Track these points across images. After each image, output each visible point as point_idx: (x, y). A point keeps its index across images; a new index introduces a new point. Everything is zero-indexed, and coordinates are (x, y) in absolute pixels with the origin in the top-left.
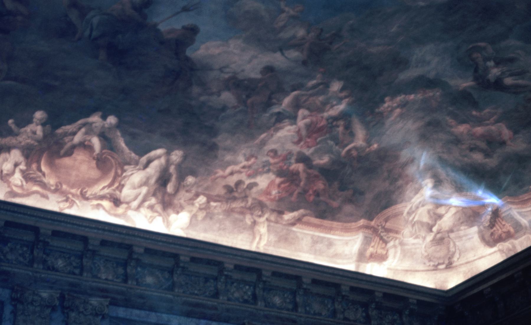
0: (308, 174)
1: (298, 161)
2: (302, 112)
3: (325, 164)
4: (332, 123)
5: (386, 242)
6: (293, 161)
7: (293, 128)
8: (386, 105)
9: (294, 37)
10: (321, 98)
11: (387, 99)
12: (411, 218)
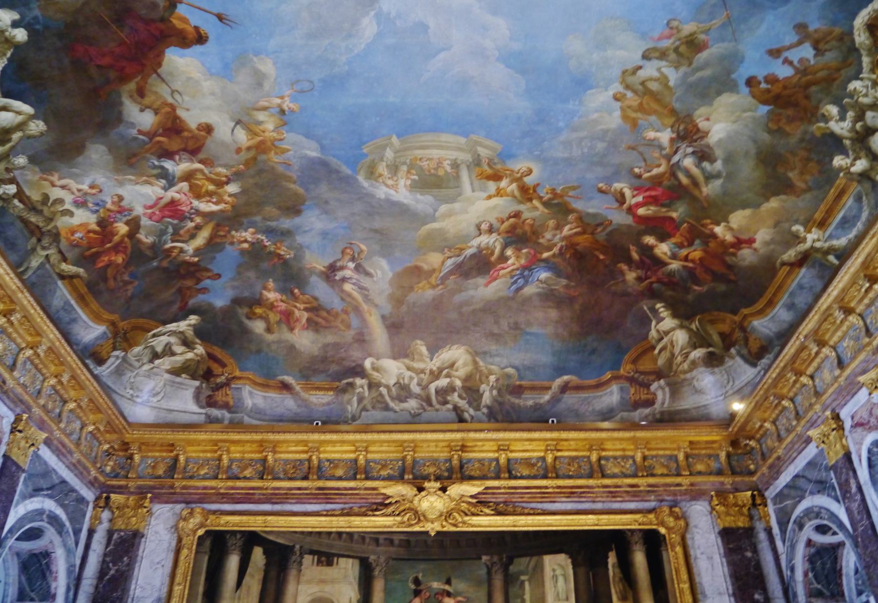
0: (122, 241)
1: (127, 223)
2: (184, 185)
6: (125, 219)
7: (160, 192)
8: (244, 234)
9: (260, 123)
10: (211, 187)
11: (251, 230)
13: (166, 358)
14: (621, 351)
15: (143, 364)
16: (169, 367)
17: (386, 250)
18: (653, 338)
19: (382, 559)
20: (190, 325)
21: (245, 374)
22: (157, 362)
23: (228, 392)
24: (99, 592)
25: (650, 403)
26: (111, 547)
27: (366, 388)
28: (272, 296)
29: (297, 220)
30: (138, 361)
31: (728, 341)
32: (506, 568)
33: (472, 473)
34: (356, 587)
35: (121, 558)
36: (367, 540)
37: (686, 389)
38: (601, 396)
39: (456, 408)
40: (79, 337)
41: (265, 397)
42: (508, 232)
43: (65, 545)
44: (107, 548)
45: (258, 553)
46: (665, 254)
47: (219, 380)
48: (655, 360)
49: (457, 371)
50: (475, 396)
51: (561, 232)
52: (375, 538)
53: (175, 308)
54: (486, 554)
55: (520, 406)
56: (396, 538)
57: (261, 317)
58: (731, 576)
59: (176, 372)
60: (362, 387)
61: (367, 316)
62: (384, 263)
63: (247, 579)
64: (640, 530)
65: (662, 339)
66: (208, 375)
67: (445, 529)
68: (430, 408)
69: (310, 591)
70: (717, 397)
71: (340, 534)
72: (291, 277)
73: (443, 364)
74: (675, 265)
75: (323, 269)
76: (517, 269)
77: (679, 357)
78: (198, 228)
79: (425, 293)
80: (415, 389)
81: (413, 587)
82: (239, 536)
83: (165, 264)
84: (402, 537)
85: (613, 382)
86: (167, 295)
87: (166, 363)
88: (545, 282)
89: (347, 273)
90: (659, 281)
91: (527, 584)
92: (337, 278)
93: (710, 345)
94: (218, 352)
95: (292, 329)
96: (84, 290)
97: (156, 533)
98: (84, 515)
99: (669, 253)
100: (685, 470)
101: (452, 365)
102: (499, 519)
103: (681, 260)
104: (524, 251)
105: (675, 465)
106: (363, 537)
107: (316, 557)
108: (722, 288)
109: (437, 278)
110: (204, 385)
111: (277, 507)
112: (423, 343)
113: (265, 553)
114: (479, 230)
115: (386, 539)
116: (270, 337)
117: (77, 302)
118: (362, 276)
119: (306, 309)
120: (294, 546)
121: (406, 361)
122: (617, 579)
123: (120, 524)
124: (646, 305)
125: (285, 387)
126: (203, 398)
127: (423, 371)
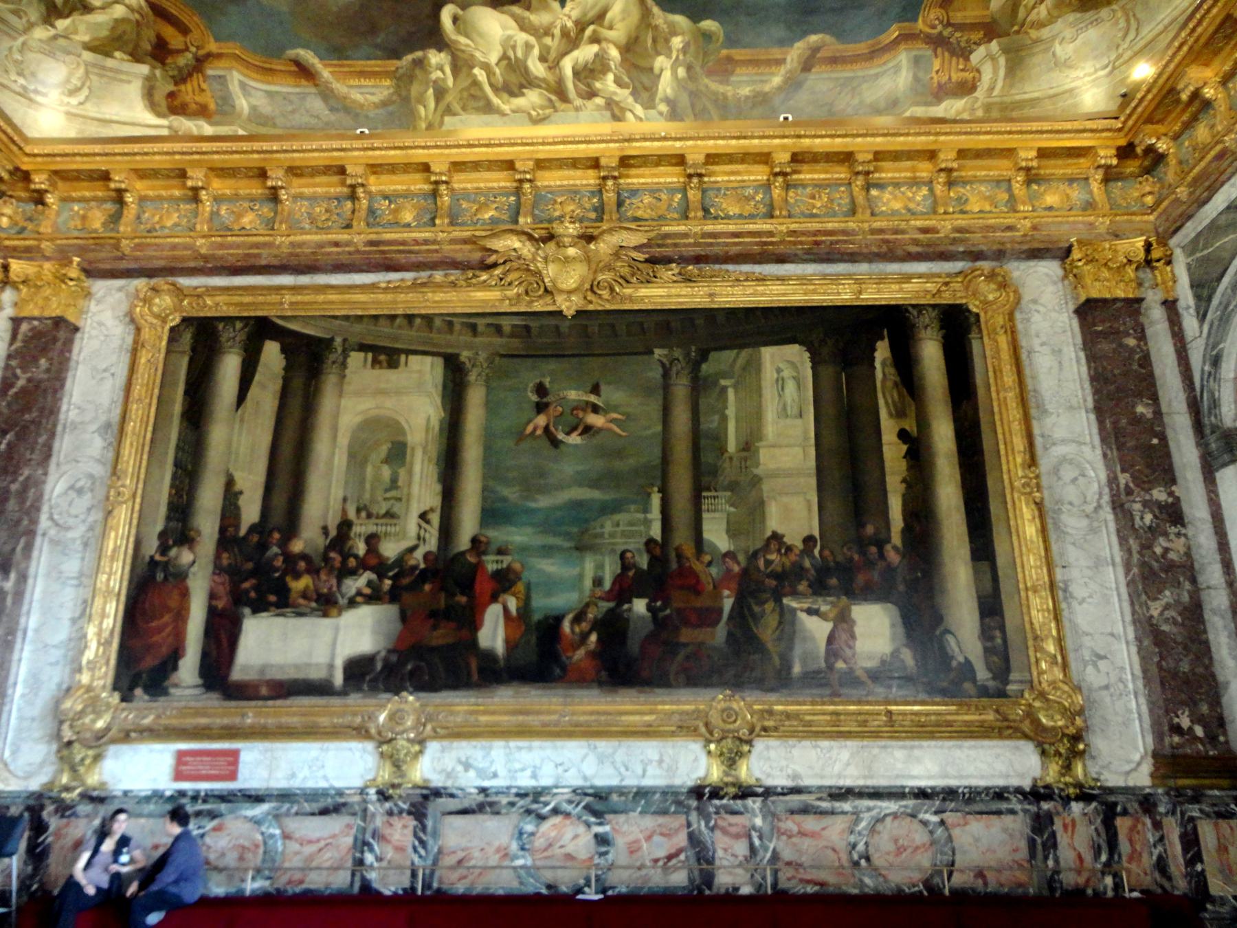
13: (76, 17)
16: (86, 38)
19: (483, 356)
22: (62, 24)
23: (204, 86)
25: (966, 88)
27: (448, 70)
30: (16, 13)
32: (696, 366)
33: (639, 213)
34: (438, 401)
35: (35, 360)
36: (457, 327)
37: (1037, 59)
38: (877, 76)
39: (610, 104)
41: (270, 94)
44: (11, 344)
45: (272, 352)
47: (184, 60)
49: (611, 28)
50: (645, 79)
52: (471, 322)
54: (662, 347)
55: (725, 98)
56: (506, 323)
59: (102, 48)
60: (442, 69)
64: (934, 306)
66: (160, 52)
67: (591, 307)
68: (564, 106)
70: (1096, 71)
71: (410, 318)
73: (585, 14)
80: (537, 68)
81: (535, 398)
82: (239, 325)
84: (517, 321)
85: (902, 46)
91: (731, 393)
97: (100, 324)
100: (1024, 203)
101: (600, 18)
105: (1006, 196)
106: (449, 321)
107: (370, 355)
110: (158, 72)
111: (304, 280)
113: (283, 350)
120: (332, 339)
121: (516, 9)
122: (889, 384)
123: (32, 310)
125: (304, 71)
126: (160, 96)
127: (548, 32)
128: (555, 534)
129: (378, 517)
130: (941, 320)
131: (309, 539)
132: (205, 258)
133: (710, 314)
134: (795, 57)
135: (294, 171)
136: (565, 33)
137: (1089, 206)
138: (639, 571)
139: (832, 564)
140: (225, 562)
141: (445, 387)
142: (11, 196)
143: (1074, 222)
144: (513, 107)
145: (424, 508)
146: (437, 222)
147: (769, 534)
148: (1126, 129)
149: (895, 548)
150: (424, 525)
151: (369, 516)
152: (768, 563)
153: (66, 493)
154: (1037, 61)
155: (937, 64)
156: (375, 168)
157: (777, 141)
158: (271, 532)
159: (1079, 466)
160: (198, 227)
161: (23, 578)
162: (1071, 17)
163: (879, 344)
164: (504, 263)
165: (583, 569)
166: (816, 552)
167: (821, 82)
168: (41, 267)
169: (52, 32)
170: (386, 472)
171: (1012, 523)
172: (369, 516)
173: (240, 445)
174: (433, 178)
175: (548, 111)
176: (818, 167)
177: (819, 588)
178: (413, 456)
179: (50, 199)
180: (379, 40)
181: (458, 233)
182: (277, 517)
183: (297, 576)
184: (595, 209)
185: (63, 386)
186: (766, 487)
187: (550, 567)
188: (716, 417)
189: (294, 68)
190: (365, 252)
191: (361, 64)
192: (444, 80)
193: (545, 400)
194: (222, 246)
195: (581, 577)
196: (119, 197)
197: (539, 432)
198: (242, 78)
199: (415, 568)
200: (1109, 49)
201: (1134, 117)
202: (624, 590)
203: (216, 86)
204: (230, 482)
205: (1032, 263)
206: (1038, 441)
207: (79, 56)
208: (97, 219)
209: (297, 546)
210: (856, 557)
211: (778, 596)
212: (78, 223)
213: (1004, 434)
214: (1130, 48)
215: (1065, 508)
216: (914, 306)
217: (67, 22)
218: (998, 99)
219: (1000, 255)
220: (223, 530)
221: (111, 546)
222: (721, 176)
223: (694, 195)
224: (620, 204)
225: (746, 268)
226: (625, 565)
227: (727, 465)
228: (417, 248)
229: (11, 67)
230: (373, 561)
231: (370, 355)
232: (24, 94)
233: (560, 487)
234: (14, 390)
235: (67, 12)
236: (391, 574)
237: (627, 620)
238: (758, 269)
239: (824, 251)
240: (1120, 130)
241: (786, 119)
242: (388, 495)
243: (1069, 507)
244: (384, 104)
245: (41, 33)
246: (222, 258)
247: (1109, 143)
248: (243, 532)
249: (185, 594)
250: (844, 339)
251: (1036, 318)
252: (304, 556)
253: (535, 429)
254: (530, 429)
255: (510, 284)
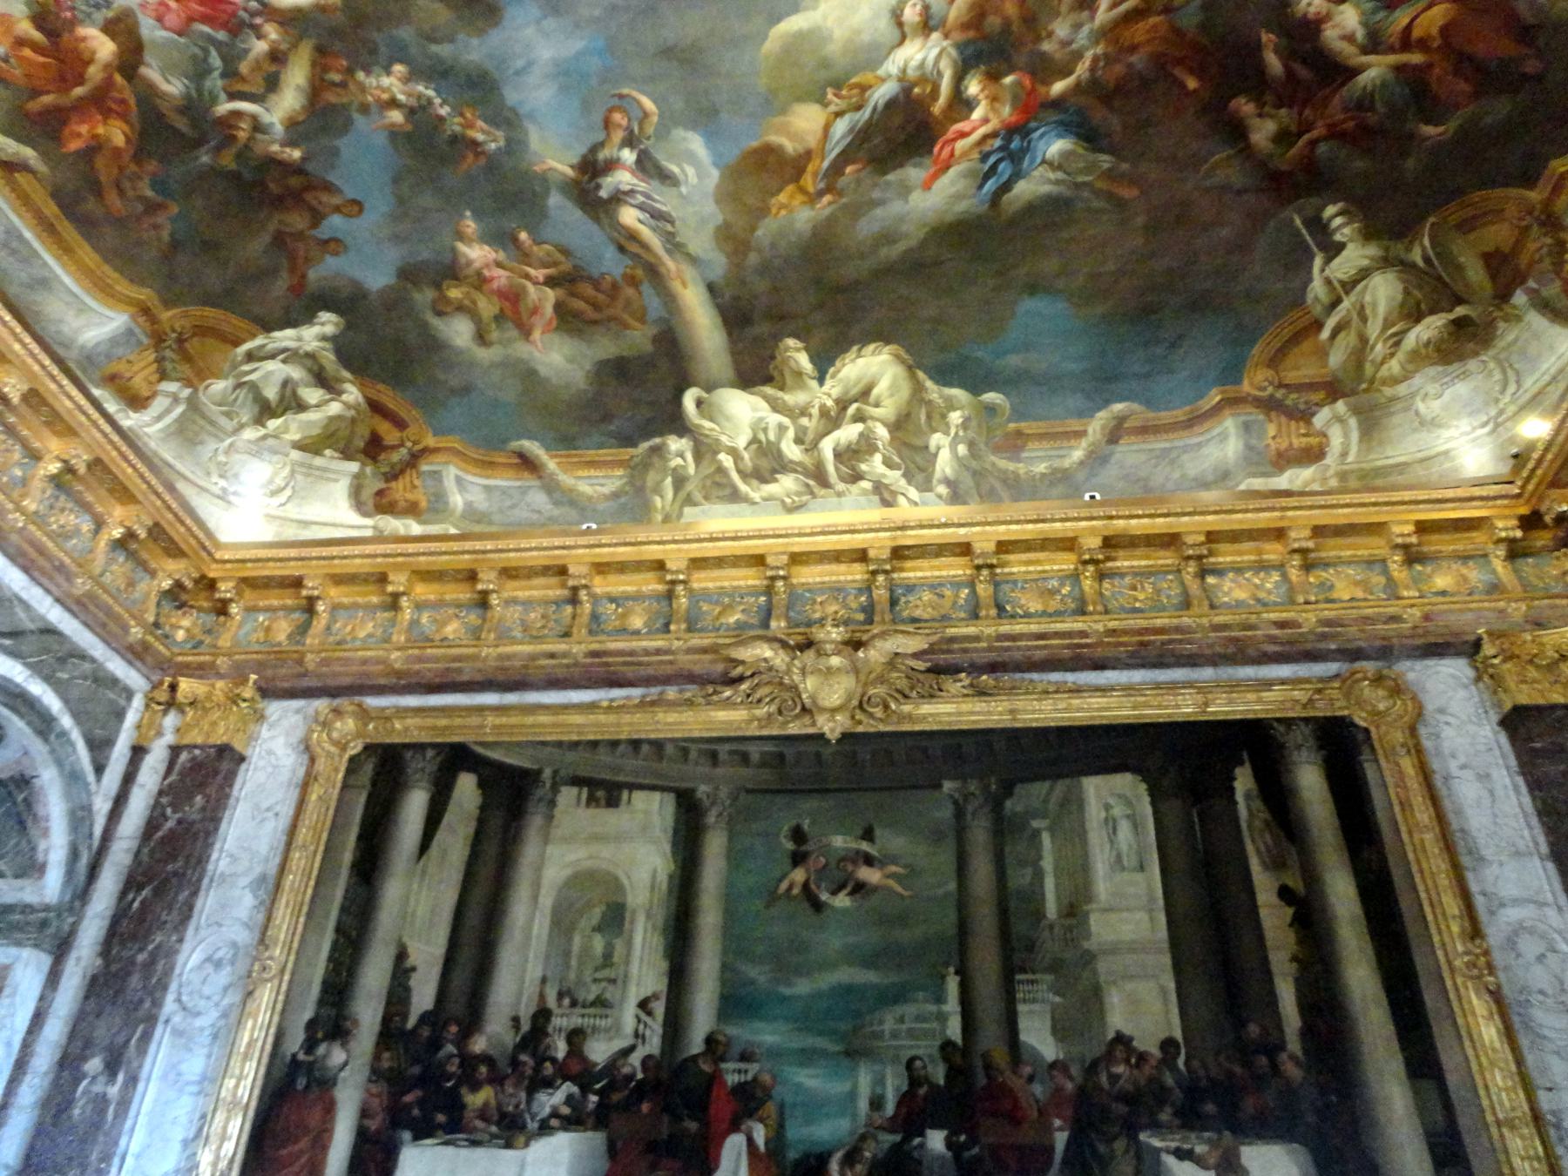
0: (108, 84)
1: (109, 28)
3: (163, 96)
4: (253, 14)
5: (163, 376)
8: (386, 81)
11: (399, 68)
12: (246, 368)
13: (289, 416)
14: (1243, 338)
15: (242, 427)
16: (297, 437)
17: (704, 117)
18: (1316, 299)
19: (724, 792)
20: (324, 338)
21: (444, 443)
22: (273, 424)
23: (416, 482)
24: (140, 863)
25: (1313, 455)
26: (173, 778)
27: (689, 456)
28: (477, 254)
29: (495, 37)
30: (228, 415)
31: (1506, 273)
33: (918, 613)
34: (667, 848)
35: (190, 797)
36: (693, 755)
37: (1396, 420)
38: (1200, 445)
40: (65, 329)
41: (487, 488)
42: (965, 26)
43: (59, 763)
45: (466, 787)
46: (1350, 38)
47: (396, 457)
48: (1322, 353)
49: (877, 405)
51: (1092, 18)
52: (712, 750)
53: (282, 284)
56: (755, 751)
57: (460, 308)
58: (1540, 814)
59: (310, 446)
60: (681, 455)
61: (676, 286)
62: (696, 143)
63: (441, 836)
64: (1306, 720)
65: (1336, 302)
66: (373, 448)
67: (860, 729)
68: (823, 492)
69: (572, 857)
70: (1474, 429)
71: (636, 744)
72: (510, 196)
73: (846, 393)
74: (1375, 71)
75: (570, 172)
76: (993, 135)
77: (1379, 347)
78: (277, 57)
79: (796, 214)
80: (792, 451)
81: (790, 846)
83: (228, 161)
84: (769, 748)
85: (1227, 412)
86: (255, 247)
87: (293, 427)
88: (1059, 167)
89: (623, 178)
90: (1334, 134)
91: (1046, 839)
92: (603, 194)
93: (1459, 301)
94: (388, 397)
95: (526, 333)
96: (51, 209)
97: (270, 752)
98: (120, 715)
99: (1360, 35)
100: (1407, 588)
101: (865, 394)
102: (979, 705)
103: (1392, 50)
104: (1008, 80)
105: (1383, 580)
106: (684, 747)
107: (585, 791)
108: (1499, 109)
109: (815, 174)
110: (368, 470)
111: (511, 698)
112: (800, 345)
113: (482, 784)
114: (900, 25)
115: (731, 753)
116: (483, 354)
117: (39, 237)
118: (655, 183)
119: (551, 282)
120: (539, 772)
121: (768, 390)
122: (1257, 823)
124: (1299, 212)
125: (527, 463)
126: (368, 493)
127: (804, 412)
128: (820, 1033)
129: (584, 1007)
130: (1318, 738)
131: (495, 1033)
132: (399, 674)
133: (1014, 737)
134: (1098, 428)
135: (508, 573)
136: (824, 412)
137: (1495, 588)
138: (933, 1087)
139: (1204, 1083)
140: (386, 1064)
141: (676, 831)
142: (192, 607)
143: (1480, 609)
144: (764, 494)
145: (646, 991)
146: (672, 627)
147: (1111, 1035)
148: (1526, 495)
149: (1292, 1057)
150: (643, 1016)
151: (574, 1004)
152: (1114, 1078)
153: (200, 967)
154: (1398, 421)
155: (1271, 430)
156: (601, 568)
157: (1084, 524)
158: (446, 1024)
159: (1543, 937)
160: (395, 638)
161: (133, 1080)
162: (1432, 371)
163: (1238, 771)
164: (752, 675)
165: (855, 1086)
166: (1181, 1062)
167: (1130, 454)
168: (213, 686)
169: (262, 432)
170: (598, 944)
171: (1460, 1021)
172: (574, 1004)
173: (418, 906)
174: (669, 577)
175: (805, 498)
176: (1138, 552)
177: (1190, 1119)
178: (632, 922)
179: (234, 609)
180: (612, 428)
181: (696, 641)
182: (457, 1007)
183: (475, 1087)
184: (863, 609)
185: (216, 829)
186: (1102, 966)
187: (809, 1079)
188: (1029, 871)
189: (517, 461)
190: (584, 666)
191: (591, 454)
192: (684, 467)
193: (803, 848)
194: (420, 660)
195: (852, 1096)
196: (309, 607)
197: (796, 891)
198: (460, 473)
199: (631, 1077)
200: (1487, 404)
201: (1534, 481)
202: (915, 1113)
203: (429, 482)
204: (401, 955)
205: (1430, 662)
206: (1480, 902)
207: (287, 455)
208: (282, 630)
209: (479, 1045)
210: (1238, 1070)
211: (1131, 1130)
212: (261, 635)
213: (1427, 891)
214: (1512, 402)
215: (1535, 999)
216: (1278, 720)
217: (279, 421)
218: (1355, 466)
219: (1385, 652)
220: (386, 1020)
221: (246, 1039)
222: (1017, 566)
223: (984, 590)
224: (893, 602)
225: (1056, 677)
226: (915, 1081)
227: (1046, 933)
228: (646, 659)
229: (213, 468)
230: (576, 1068)
231: (585, 791)
232: (223, 497)
233: (827, 965)
234: (160, 834)
235: (280, 411)
236: (598, 1086)
237: (920, 1163)
238: (1071, 678)
239: (1151, 653)
240: (1518, 496)
241: (1092, 497)
242: (598, 975)
243: (1541, 997)
244: (615, 495)
245: (250, 434)
246: (418, 672)
247: (1507, 512)
248: (411, 1022)
249: (330, 1109)
250: (1190, 766)
251: (1447, 732)
252: (487, 1059)
253: (790, 887)
254: (784, 886)
255: (759, 701)
